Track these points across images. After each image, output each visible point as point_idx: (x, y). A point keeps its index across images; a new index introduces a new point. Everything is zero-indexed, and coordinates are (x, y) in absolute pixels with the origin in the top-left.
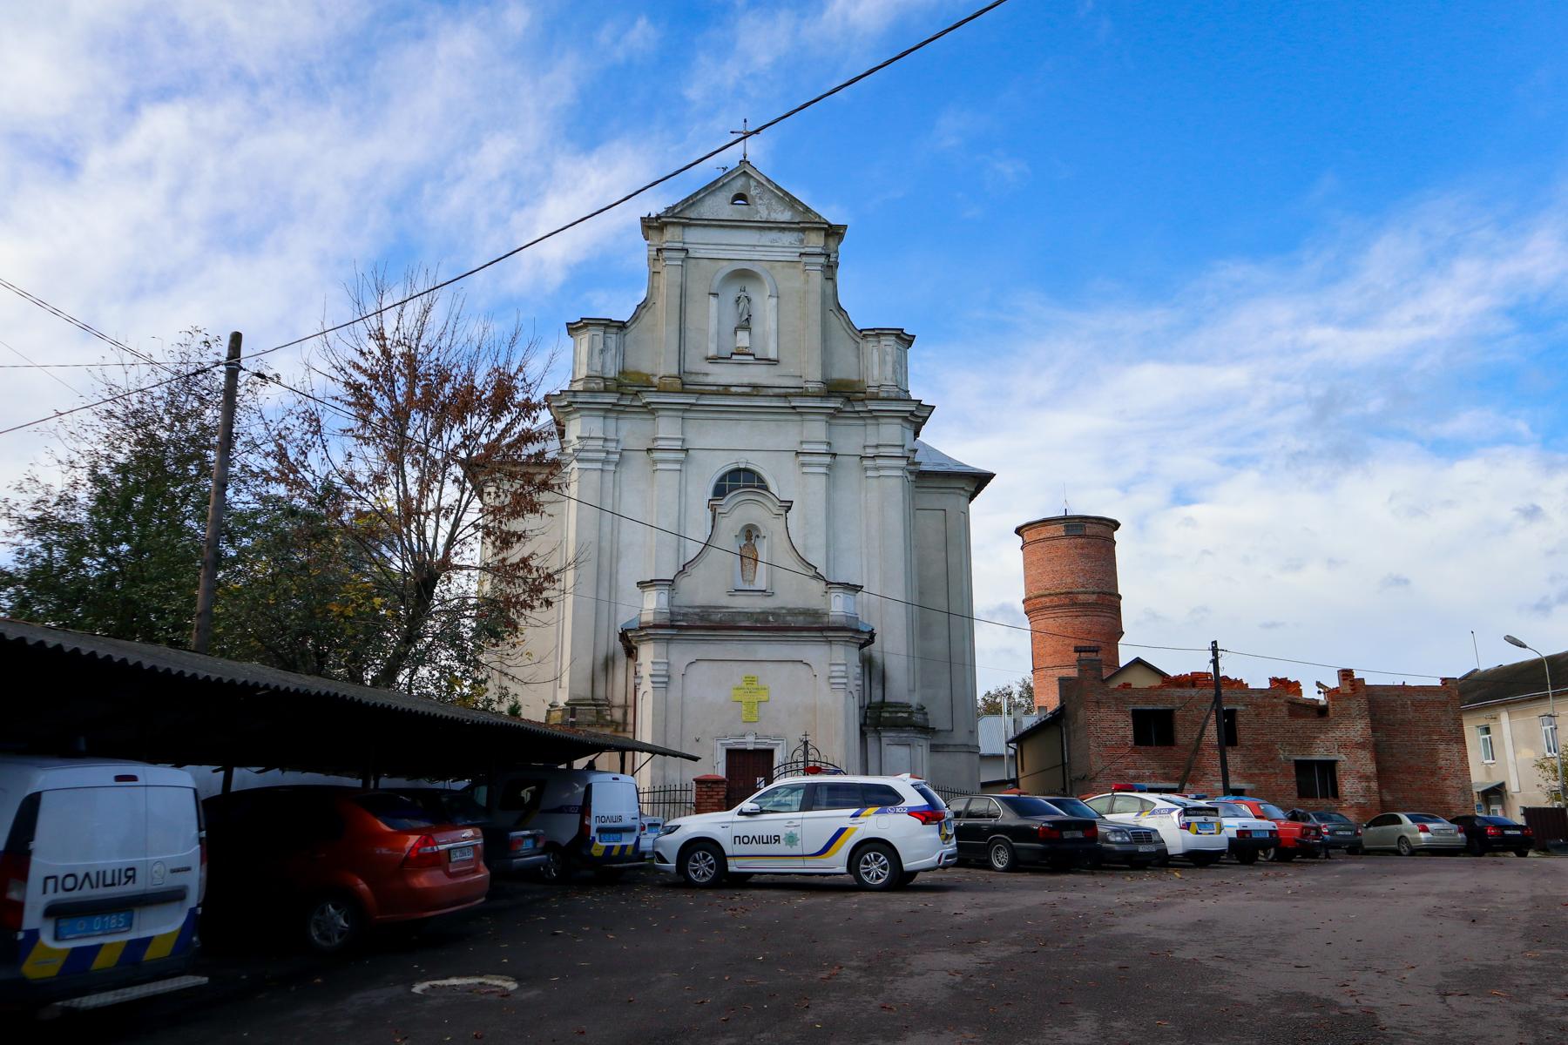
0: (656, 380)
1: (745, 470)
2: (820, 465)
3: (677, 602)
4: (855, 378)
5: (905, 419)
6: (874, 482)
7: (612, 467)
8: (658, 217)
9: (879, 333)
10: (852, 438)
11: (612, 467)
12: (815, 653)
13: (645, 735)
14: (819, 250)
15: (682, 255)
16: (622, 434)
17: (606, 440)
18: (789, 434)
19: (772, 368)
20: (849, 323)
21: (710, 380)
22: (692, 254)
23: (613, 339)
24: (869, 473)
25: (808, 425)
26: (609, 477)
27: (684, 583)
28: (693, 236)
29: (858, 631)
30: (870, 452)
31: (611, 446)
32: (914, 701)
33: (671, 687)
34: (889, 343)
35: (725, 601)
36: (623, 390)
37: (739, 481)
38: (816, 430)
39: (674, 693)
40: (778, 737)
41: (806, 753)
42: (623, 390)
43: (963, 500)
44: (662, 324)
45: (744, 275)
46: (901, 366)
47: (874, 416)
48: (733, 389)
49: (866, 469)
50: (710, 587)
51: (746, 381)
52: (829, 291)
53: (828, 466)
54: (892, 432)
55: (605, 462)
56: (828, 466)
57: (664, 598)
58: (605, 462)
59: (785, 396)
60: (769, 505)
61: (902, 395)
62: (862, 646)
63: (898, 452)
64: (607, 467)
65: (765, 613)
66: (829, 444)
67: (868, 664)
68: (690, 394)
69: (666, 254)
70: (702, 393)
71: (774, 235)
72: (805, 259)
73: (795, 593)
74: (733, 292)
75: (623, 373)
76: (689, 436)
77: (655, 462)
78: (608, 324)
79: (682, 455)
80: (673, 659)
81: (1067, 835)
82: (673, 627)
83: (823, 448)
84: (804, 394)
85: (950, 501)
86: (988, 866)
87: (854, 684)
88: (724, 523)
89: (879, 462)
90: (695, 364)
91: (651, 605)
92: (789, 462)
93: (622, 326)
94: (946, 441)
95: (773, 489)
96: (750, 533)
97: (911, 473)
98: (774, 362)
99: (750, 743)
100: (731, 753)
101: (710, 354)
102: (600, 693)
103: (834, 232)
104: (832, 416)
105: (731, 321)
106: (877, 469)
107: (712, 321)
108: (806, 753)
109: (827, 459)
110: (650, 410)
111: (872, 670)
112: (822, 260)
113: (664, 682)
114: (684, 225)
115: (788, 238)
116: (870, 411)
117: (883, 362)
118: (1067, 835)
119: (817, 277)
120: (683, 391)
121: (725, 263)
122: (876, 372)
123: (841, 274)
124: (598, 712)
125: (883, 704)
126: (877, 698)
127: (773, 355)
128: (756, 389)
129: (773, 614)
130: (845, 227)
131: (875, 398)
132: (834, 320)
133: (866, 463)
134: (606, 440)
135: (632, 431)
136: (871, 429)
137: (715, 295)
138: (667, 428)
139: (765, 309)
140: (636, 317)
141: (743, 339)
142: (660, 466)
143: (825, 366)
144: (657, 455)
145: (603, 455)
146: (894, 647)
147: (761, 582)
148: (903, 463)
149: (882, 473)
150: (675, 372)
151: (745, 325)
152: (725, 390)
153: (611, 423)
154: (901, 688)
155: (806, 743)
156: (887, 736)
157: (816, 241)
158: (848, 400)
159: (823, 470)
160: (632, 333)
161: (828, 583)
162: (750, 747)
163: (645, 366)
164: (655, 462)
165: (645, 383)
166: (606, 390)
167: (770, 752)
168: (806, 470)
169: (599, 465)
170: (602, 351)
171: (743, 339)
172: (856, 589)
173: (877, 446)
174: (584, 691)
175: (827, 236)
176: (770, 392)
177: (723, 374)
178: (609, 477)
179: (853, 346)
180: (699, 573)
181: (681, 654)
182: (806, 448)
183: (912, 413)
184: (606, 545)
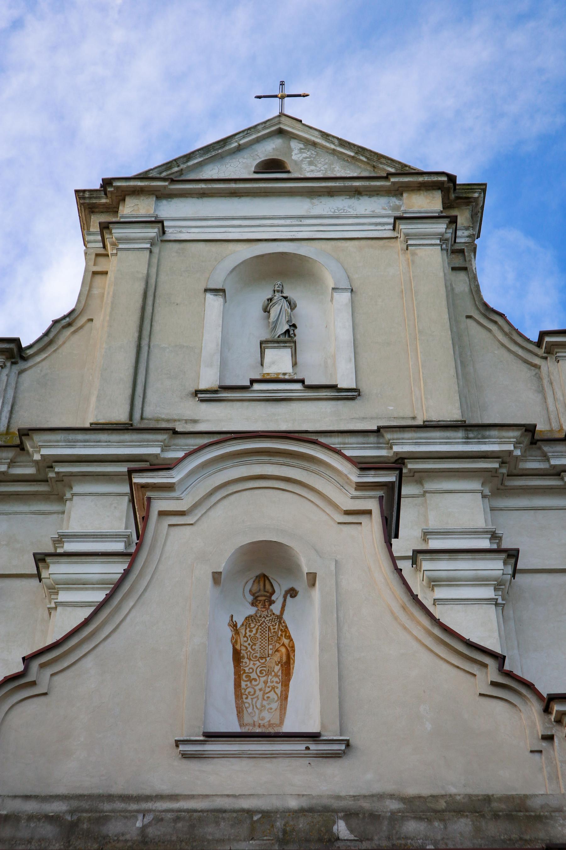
2: (479, 581)
15: (152, 232)
20: (513, 333)
22: (171, 234)
44: (106, 349)
53: (499, 585)
72: (403, 227)
77: (53, 590)
101: (208, 379)
107: (212, 337)
109: (495, 566)
119: (433, 258)
127: (345, 381)
129: (349, 815)
130: (483, 188)
132: (476, 333)
141: (279, 361)
142: (63, 596)
147: (305, 710)
159: (488, 593)
171: (279, 361)
179: (525, 372)
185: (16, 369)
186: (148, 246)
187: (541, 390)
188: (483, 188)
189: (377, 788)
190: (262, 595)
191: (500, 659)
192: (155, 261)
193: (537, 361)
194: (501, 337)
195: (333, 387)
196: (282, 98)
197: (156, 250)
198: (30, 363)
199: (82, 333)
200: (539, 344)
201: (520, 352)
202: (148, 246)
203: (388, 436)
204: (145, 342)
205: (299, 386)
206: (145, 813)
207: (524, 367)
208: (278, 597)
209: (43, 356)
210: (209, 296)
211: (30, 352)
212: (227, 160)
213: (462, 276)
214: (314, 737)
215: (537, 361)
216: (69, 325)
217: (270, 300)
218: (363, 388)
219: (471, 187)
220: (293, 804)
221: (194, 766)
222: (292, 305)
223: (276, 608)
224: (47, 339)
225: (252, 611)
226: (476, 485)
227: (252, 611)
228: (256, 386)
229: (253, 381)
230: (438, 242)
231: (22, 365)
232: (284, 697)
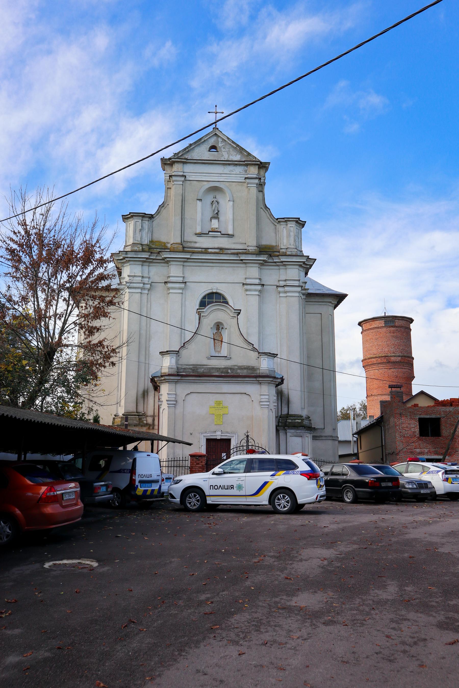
0: (169, 246)
1: (216, 293)
2: (255, 290)
3: (180, 362)
4: (274, 244)
5: (300, 266)
6: (284, 299)
7: (146, 292)
8: (170, 159)
9: (286, 220)
10: (272, 276)
11: (146, 292)
12: (253, 389)
13: (164, 432)
14: (255, 176)
15: (183, 179)
16: (151, 274)
17: (143, 277)
18: (239, 274)
19: (230, 239)
20: (271, 215)
21: (197, 245)
22: (188, 178)
23: (146, 224)
24: (281, 295)
25: (249, 269)
26: (145, 297)
27: (184, 353)
28: (188, 168)
29: (275, 378)
30: (282, 283)
31: (146, 280)
32: (304, 413)
33: (177, 407)
34: (292, 225)
35: (205, 362)
36: (152, 250)
37: (212, 299)
38: (253, 272)
39: (179, 409)
40: (232, 433)
41: (248, 441)
42: (152, 250)
43: (331, 308)
45: (215, 189)
46: (298, 238)
47: (284, 264)
48: (210, 250)
49: (280, 293)
50: (198, 354)
51: (216, 246)
52: (260, 197)
53: (260, 291)
54: (293, 273)
55: (142, 289)
56: (260, 291)
57: (174, 361)
58: (142, 289)
59: (237, 254)
60: (229, 312)
61: (299, 253)
62: (277, 386)
63: (296, 283)
64: (144, 292)
65: (226, 368)
66: (260, 279)
67: (280, 394)
68: (187, 253)
69: (174, 178)
70: (193, 253)
71: (231, 168)
72: (248, 181)
73: (242, 358)
74: (209, 198)
75: (152, 242)
76: (187, 275)
77: (169, 289)
78: (144, 216)
79: (182, 285)
80: (179, 392)
81: (383, 484)
82: (178, 375)
83: (257, 281)
84: (247, 253)
85: (324, 309)
86: (343, 501)
87: (273, 405)
88: (205, 321)
89: (287, 289)
90: (190, 237)
91: (167, 364)
92: (239, 289)
93: (151, 217)
94: (324, 277)
95: (231, 303)
96: (219, 326)
97: (303, 294)
98: (231, 236)
99: (218, 436)
100: (208, 441)
101: (198, 231)
102: (141, 409)
103: (263, 166)
104: (262, 264)
105: (209, 214)
106: (286, 292)
107: (199, 214)
108: (248, 441)
109: (259, 287)
110: (166, 261)
111: (282, 397)
112: (257, 181)
113: (173, 404)
114: (184, 163)
115: (239, 169)
116: (282, 262)
117: (289, 236)
118: (383, 484)
119: (254, 190)
120: (183, 251)
121: (205, 183)
122: (285, 241)
123: (266, 189)
124: (140, 419)
125: (288, 415)
126: (285, 412)
127: (230, 232)
128: (222, 250)
129: (231, 369)
130: (269, 163)
131: (285, 255)
132: (263, 214)
133: (280, 289)
134: (143, 277)
135: (156, 272)
136: (282, 271)
137: (200, 200)
138: (175, 271)
139: (227, 208)
140: (158, 212)
141: (215, 224)
143: (258, 237)
144: (169, 285)
145: (141, 285)
146: (294, 386)
147: (224, 352)
148: (299, 289)
149: (288, 294)
150: (179, 241)
151: (216, 216)
152: (205, 251)
153: (146, 268)
154: (297, 407)
155: (248, 436)
156: (290, 432)
157: (253, 171)
158: (270, 256)
160: (156, 221)
161: (259, 353)
162: (219, 438)
163: (163, 239)
164: (169, 289)
165: (163, 247)
166: (143, 251)
167: (229, 441)
168: (248, 293)
169: (139, 291)
170: (141, 230)
171: (215, 224)
172: (274, 355)
173: (285, 280)
174: (132, 408)
175: (259, 168)
176: (229, 252)
177: (204, 242)
178: (145, 297)
179: (273, 227)
180: (192, 347)
181: (183, 389)
182: (248, 281)
183: (304, 263)
184: (143, 332)
185: (151, 220)
186: (182, 183)
187: (276, 233)
188: (269, 163)
189: (234, 364)
190: (218, 329)
191: (253, 345)
192: (184, 188)
193: (276, 224)
194: (268, 215)
195: (228, 235)
196: (216, 113)
197: (184, 184)
198: (155, 219)
199: (166, 209)
200: (277, 219)
201: (272, 221)
202: (182, 183)
203: (239, 255)
204: (183, 217)
205: (219, 234)
206: (203, 368)
207: (273, 225)
208: (220, 329)
209: (157, 216)
210: (198, 201)
211: (154, 216)
212: (201, 145)
213: (261, 193)
214: (226, 357)
215: (276, 224)
216: (163, 206)
217: (213, 202)
218: (235, 234)
219: (266, 163)
220: (223, 367)
221: (209, 360)
222: (218, 203)
223: (220, 331)
224: (158, 212)
225: (216, 331)
226: (257, 265)
227: (216, 331)
228: (210, 233)
229: (209, 232)
230: (255, 185)
231: (152, 219)
232: (221, 347)
